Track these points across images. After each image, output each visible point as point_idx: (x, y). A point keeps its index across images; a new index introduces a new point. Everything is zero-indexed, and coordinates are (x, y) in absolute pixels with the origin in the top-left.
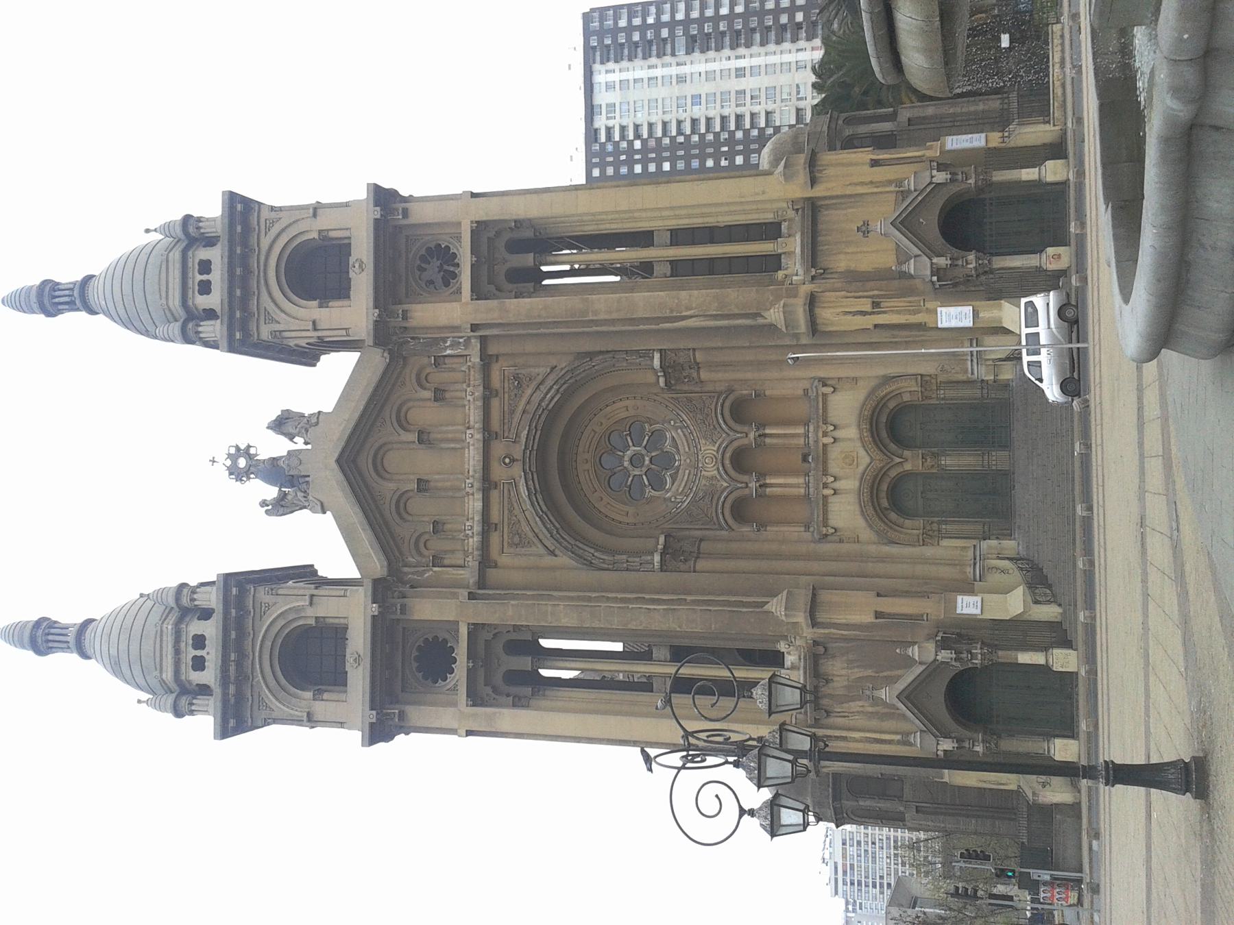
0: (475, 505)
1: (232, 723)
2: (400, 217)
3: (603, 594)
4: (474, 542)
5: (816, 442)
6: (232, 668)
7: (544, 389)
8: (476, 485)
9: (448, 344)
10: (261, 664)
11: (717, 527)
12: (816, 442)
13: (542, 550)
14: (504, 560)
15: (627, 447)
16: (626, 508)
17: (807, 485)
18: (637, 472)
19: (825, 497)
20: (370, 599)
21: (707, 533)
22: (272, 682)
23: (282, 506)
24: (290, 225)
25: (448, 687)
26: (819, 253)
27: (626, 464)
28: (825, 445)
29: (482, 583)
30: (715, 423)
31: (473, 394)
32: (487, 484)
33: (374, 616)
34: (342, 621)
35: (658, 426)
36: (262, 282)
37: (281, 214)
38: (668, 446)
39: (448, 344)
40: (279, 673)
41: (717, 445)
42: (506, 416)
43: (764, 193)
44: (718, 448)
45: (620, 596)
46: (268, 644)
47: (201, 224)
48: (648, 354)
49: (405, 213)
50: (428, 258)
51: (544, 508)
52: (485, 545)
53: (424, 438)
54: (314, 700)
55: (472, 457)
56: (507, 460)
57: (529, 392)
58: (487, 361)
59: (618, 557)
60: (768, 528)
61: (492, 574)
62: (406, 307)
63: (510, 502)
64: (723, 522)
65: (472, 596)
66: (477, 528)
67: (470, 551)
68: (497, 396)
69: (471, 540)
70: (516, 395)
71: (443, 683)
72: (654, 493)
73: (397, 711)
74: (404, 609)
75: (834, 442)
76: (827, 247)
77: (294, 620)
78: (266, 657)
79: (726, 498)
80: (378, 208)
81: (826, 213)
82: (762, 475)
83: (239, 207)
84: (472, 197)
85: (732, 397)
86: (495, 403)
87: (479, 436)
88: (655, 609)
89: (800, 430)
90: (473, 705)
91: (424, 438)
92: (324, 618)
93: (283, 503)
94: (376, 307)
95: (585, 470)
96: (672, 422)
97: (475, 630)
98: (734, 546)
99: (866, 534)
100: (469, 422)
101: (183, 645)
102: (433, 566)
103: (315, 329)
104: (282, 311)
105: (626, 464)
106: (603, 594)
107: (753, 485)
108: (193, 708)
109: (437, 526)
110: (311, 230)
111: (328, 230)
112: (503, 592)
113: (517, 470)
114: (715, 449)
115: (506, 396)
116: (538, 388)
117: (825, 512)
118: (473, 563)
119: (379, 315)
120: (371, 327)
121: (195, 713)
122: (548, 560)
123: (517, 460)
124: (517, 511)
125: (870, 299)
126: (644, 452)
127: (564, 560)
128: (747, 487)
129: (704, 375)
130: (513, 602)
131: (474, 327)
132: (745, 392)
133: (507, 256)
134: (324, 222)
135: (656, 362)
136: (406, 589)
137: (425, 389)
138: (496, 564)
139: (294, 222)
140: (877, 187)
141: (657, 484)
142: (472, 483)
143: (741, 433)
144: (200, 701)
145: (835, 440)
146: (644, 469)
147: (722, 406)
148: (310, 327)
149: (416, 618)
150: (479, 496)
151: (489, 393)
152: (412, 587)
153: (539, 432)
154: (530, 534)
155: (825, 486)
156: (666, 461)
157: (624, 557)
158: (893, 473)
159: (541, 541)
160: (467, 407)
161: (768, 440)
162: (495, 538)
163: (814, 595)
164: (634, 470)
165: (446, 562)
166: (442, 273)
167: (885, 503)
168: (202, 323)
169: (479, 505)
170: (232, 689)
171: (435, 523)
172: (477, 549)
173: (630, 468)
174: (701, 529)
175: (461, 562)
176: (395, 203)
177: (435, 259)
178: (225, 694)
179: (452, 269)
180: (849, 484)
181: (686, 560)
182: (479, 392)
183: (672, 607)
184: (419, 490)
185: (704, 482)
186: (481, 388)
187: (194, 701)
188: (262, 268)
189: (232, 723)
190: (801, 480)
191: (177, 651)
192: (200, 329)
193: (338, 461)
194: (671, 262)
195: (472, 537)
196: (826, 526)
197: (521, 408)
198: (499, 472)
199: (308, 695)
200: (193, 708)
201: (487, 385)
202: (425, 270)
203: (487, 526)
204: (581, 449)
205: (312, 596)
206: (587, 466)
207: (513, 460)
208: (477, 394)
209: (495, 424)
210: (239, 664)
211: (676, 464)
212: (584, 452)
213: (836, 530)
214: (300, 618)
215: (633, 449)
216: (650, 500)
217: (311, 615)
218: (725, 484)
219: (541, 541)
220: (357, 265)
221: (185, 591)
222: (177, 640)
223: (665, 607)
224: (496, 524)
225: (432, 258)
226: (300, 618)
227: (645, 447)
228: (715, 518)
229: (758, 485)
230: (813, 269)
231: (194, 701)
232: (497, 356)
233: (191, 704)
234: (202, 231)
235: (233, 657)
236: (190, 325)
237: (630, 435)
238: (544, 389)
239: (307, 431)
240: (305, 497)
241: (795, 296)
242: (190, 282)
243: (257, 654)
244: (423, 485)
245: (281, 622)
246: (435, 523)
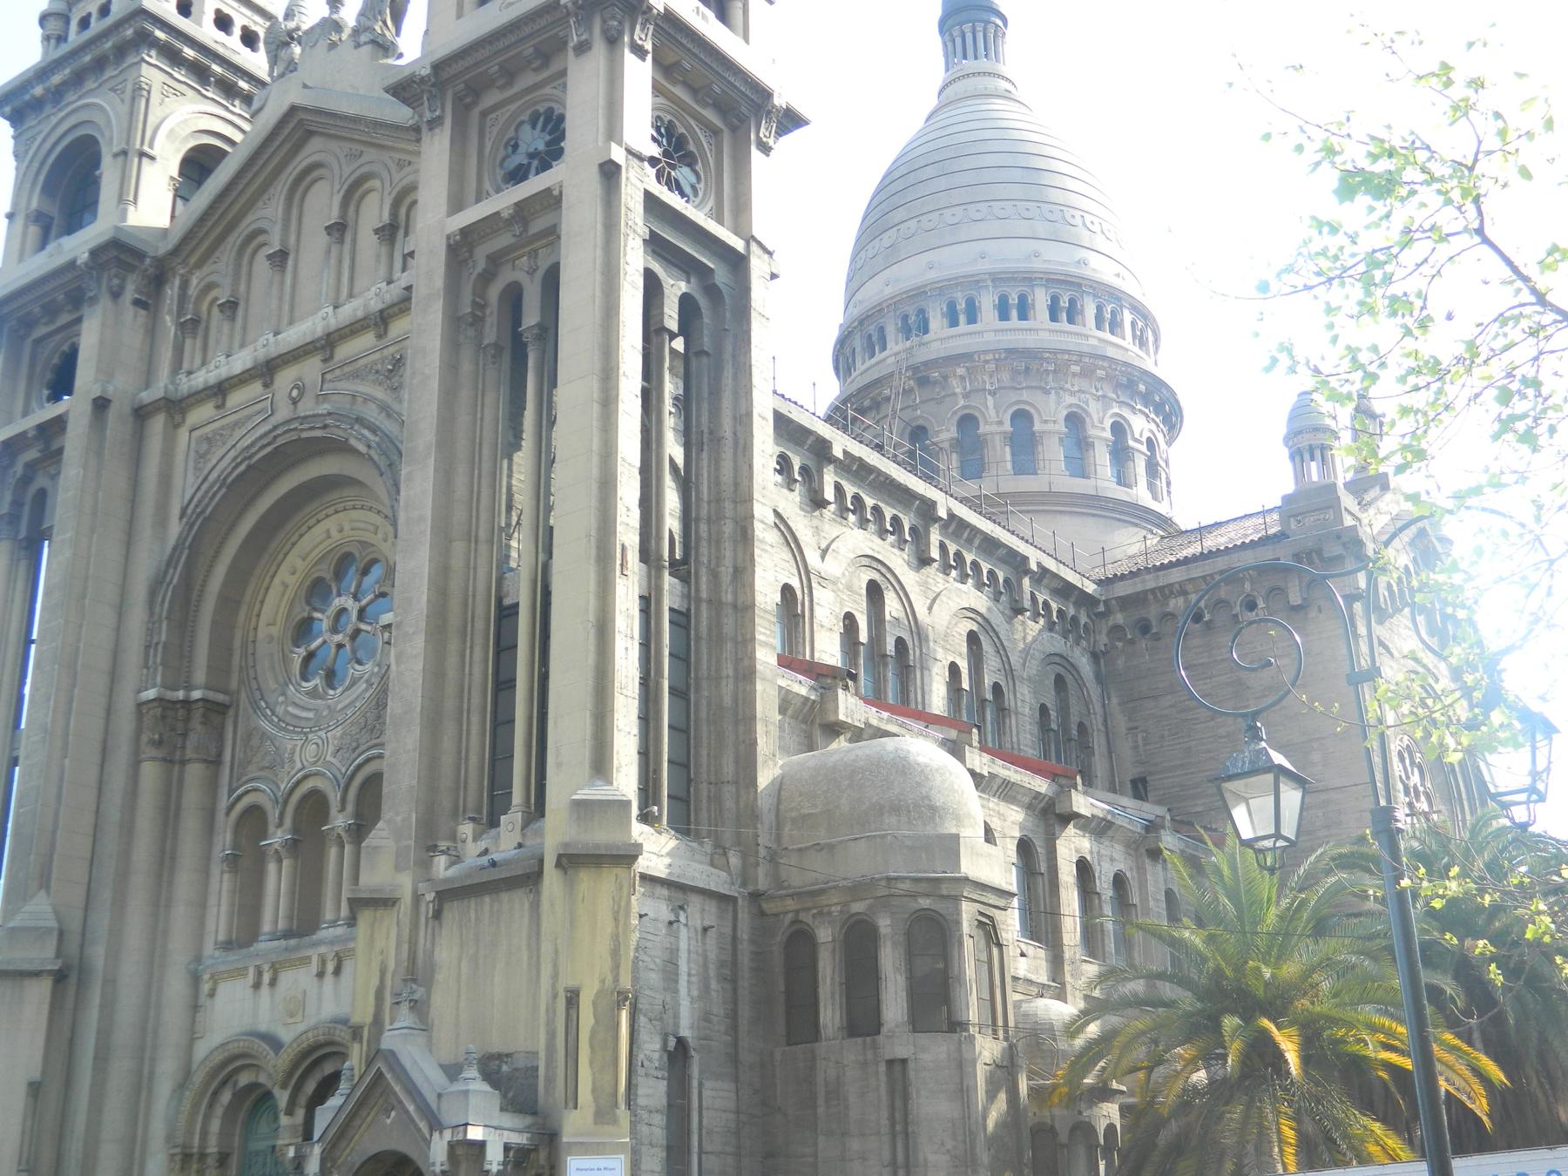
0: (241, 361)
4: (202, 378)
6: (56, 79)
10: (67, 115)
11: (235, 785)
14: (183, 435)
16: (280, 619)
20: (93, 244)
21: (227, 771)
22: (48, 146)
26: (466, 901)
29: (141, 414)
30: (362, 748)
32: (267, 370)
40: (59, 149)
42: (347, 369)
43: (559, 765)
50: (549, 127)
51: (230, 479)
54: (27, 217)
57: (380, 394)
60: (226, 877)
61: (158, 424)
63: (249, 417)
64: (239, 791)
68: (379, 337)
70: (377, 372)
71: (44, 397)
76: (473, 915)
81: (527, 906)
84: (602, 166)
86: (367, 340)
95: (328, 531)
98: (191, 823)
99: (201, 1050)
102: (182, 326)
113: (283, 412)
115: (377, 355)
122: (176, 511)
123: (296, 408)
124: (238, 433)
125: (369, 1019)
126: (349, 629)
133: (540, 274)
136: (130, 293)
138: (177, 426)
140: (547, 1010)
142: (265, 345)
152: (137, 303)
153: (318, 433)
154: (206, 472)
162: (205, 411)
163: (37, 974)
164: (328, 617)
165: (188, 342)
166: (525, 162)
170: (38, 91)
172: (190, 387)
175: (186, 366)
176: (604, 21)
177: (548, 138)
185: (289, 747)
186: (380, 306)
193: (293, 109)
194: (517, 605)
197: (364, 388)
202: (534, 127)
203: (220, 390)
204: (354, 514)
206: (334, 533)
207: (295, 402)
209: (344, 351)
210: (64, 83)
211: (331, 692)
212: (352, 521)
213: (212, 994)
216: (286, 661)
218: (282, 787)
224: (223, 404)
225: (550, 134)
227: (357, 632)
228: (245, 779)
229: (276, 846)
230: (433, 894)
231: (53, 42)
237: (377, 597)
241: (398, 868)
243: (75, 105)
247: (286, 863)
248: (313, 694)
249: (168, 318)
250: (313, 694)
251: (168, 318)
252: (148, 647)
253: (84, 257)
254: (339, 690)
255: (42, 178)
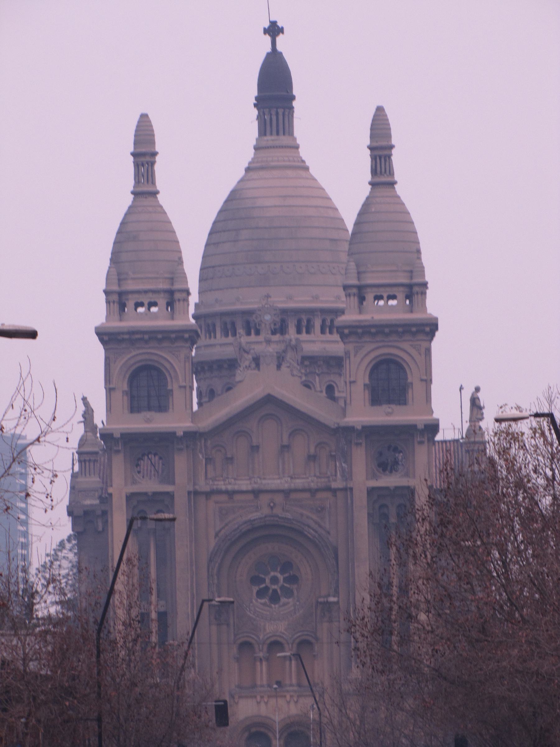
0: (244, 485)
1: (106, 338)
2: (419, 439)
3: (195, 573)
5: (288, 691)
7: (316, 527)
8: (256, 486)
9: (343, 465)
12: (288, 691)
13: (218, 529)
15: (282, 572)
17: (262, 686)
18: (268, 581)
19: (255, 697)
22: (132, 362)
23: (240, 349)
24: (416, 363)
25: (135, 476)
27: (272, 574)
28: (285, 696)
29: (196, 493)
31: (313, 481)
32: (256, 493)
33: (174, 433)
34: (171, 407)
35: (295, 592)
36: (380, 344)
37: (423, 356)
38: (283, 600)
39: (343, 465)
41: (285, 633)
44: (283, 633)
45: (194, 584)
46: (155, 358)
47: (420, 295)
48: (336, 593)
49: (421, 443)
52: (219, 492)
53: (285, 448)
54: (123, 392)
55: (274, 483)
56: (272, 504)
57: (314, 517)
58: (334, 491)
59: (215, 577)
62: (364, 445)
65: (189, 493)
66: (230, 487)
67: (216, 483)
69: (222, 483)
72: (255, 591)
73: (120, 448)
74: (180, 450)
75: (287, 701)
77: (170, 374)
78: (147, 357)
79: (253, 639)
80: (423, 427)
82: (267, 659)
83: (427, 329)
85: (313, 641)
86: (307, 495)
87: (286, 486)
88: (188, 607)
89: (294, 681)
90: (127, 496)
91: (285, 448)
92: (172, 395)
93: (242, 349)
94: (364, 427)
96: (298, 603)
97: (170, 496)
100: (295, 478)
101: (150, 295)
102: (206, 459)
103: (350, 382)
104: (362, 359)
105: (272, 574)
106: (195, 573)
107: (261, 655)
108: (112, 304)
109: (230, 460)
110: (413, 377)
111: (412, 389)
112: (193, 512)
113: (266, 511)
114: (283, 631)
116: (316, 522)
117: (246, 697)
118: (207, 489)
119: (357, 430)
120: (351, 424)
121: (108, 304)
126: (280, 584)
127: (213, 543)
128: (260, 651)
129: (326, 625)
130: (187, 520)
131: (351, 489)
132: (316, 648)
134: (417, 387)
135: (332, 599)
137: (316, 447)
139: (418, 365)
141: (261, 594)
143: (292, 647)
144: (116, 307)
145: (289, 703)
146: (269, 585)
147: (308, 635)
148: (352, 379)
149: (176, 457)
150: (250, 488)
151: (313, 492)
155: (262, 697)
156: (275, 598)
157: (216, 581)
158: (270, 735)
159: (223, 528)
160: (304, 476)
161: (288, 663)
162: (224, 498)
167: (253, 730)
168: (356, 298)
169: (244, 488)
170: (126, 337)
171: (232, 459)
173: (270, 576)
174: (234, 623)
175: (209, 476)
178: (123, 333)
179: (389, 468)
180: (264, 710)
181: (216, 619)
182: (313, 485)
183: (190, 617)
184: (252, 447)
186: (316, 487)
187: (116, 304)
188: (390, 344)
189: (106, 338)
190: (265, 682)
191: (146, 292)
192: (352, 298)
195: (224, 484)
196: (240, 697)
198: (264, 499)
199: (126, 387)
200: (112, 304)
201: (317, 490)
203: (231, 494)
205: (185, 387)
207: (272, 508)
208: (312, 484)
209: (293, 496)
211: (273, 606)
213: (237, 703)
214: (171, 378)
215: (281, 577)
217: (172, 385)
218: (261, 637)
219: (223, 528)
220: (390, 410)
221: (184, 295)
222: (154, 292)
223: (190, 613)
226: (171, 378)
231: (116, 304)
232: (336, 496)
233: (114, 302)
234: (416, 296)
235: (146, 337)
236: (355, 291)
238: (316, 527)
239: (288, 367)
240: (246, 367)
242: (382, 289)
244: (255, 449)
245: (168, 366)
246: (232, 459)
247: (264, 663)
248: (264, 604)
249: (201, 456)
250: (264, 604)
251: (201, 456)
252: (209, 584)
253: (180, 433)
254: (277, 606)
255: (128, 376)
